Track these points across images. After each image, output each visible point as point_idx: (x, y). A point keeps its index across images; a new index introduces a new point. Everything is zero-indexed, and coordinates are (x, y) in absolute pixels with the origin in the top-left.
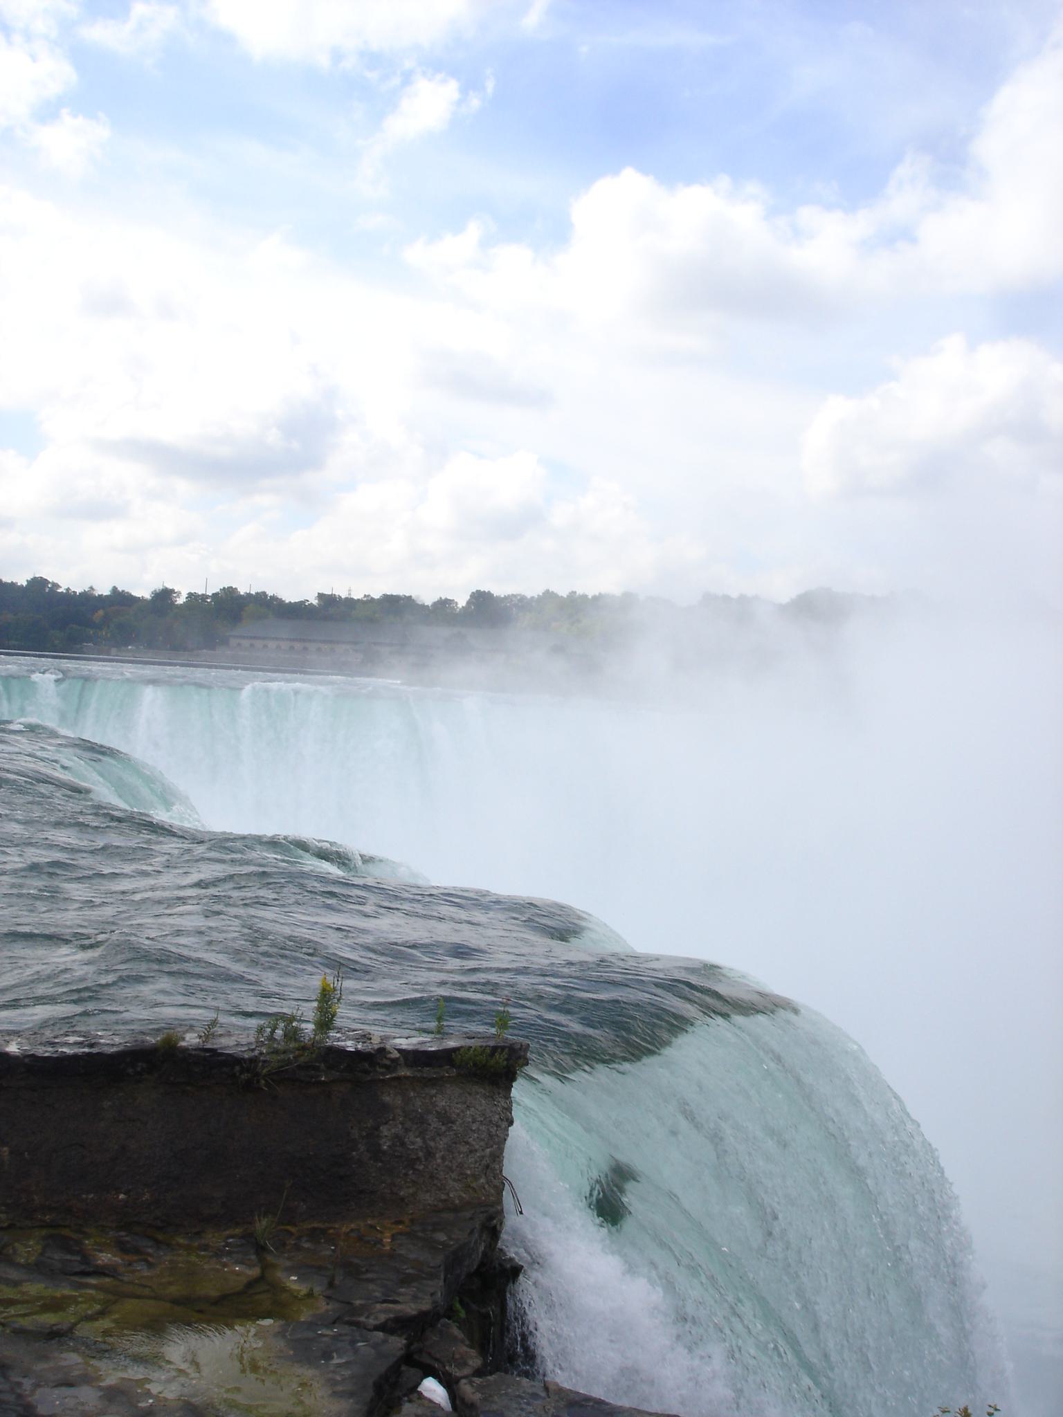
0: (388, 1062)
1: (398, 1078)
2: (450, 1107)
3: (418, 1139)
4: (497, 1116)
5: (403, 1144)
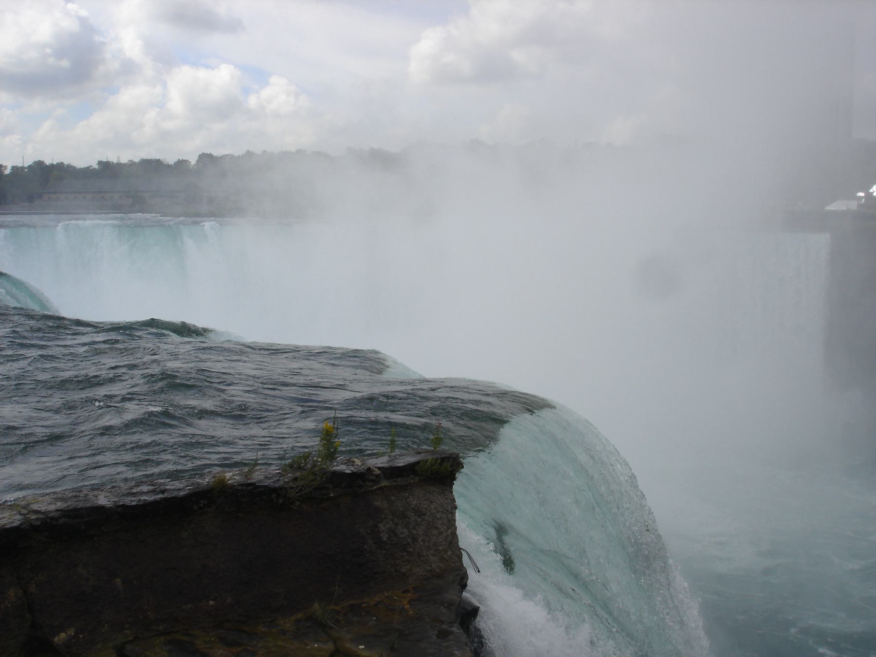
0: (374, 478)
1: (381, 488)
3: (405, 530)
4: (450, 506)
5: (396, 535)
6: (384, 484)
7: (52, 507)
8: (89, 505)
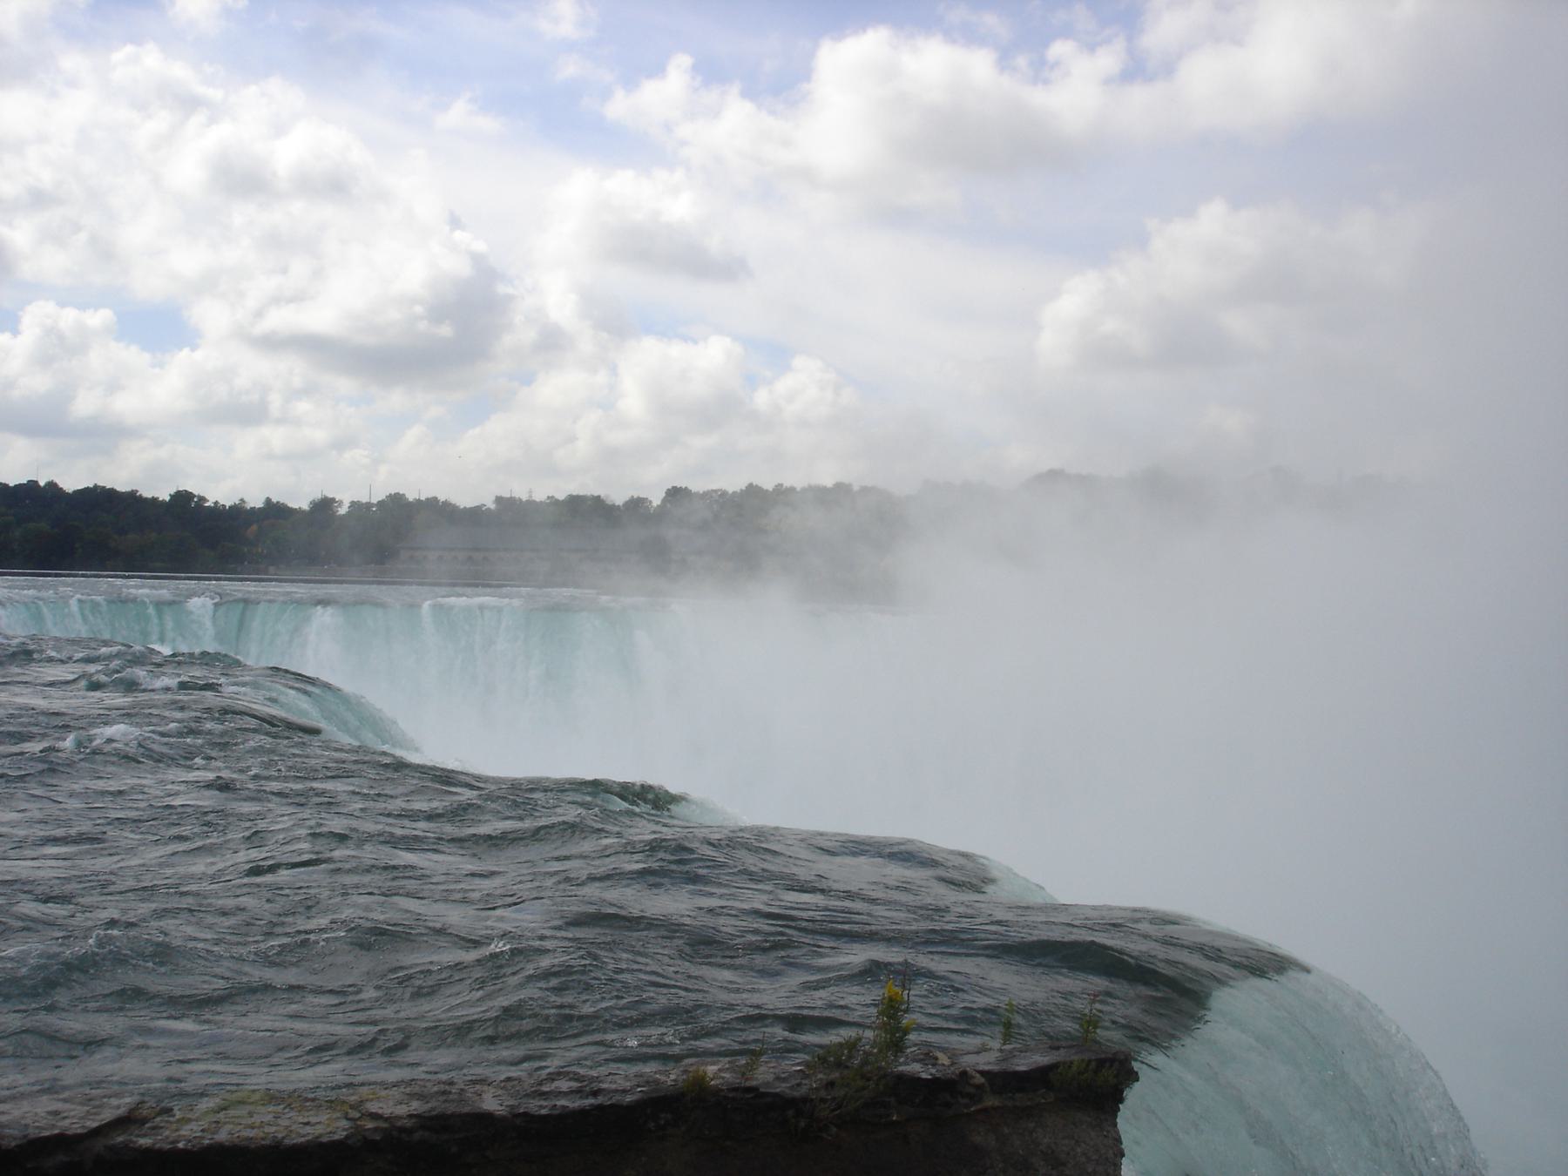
0: (972, 1090)
1: (985, 1110)
2: (1055, 1143)
4: (1111, 1152)
6: (990, 1103)
7: (402, 1110)
8: (466, 1110)
